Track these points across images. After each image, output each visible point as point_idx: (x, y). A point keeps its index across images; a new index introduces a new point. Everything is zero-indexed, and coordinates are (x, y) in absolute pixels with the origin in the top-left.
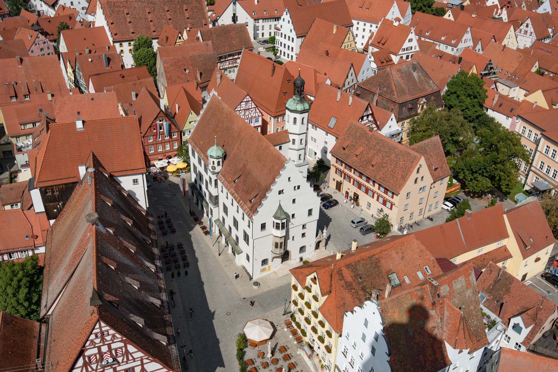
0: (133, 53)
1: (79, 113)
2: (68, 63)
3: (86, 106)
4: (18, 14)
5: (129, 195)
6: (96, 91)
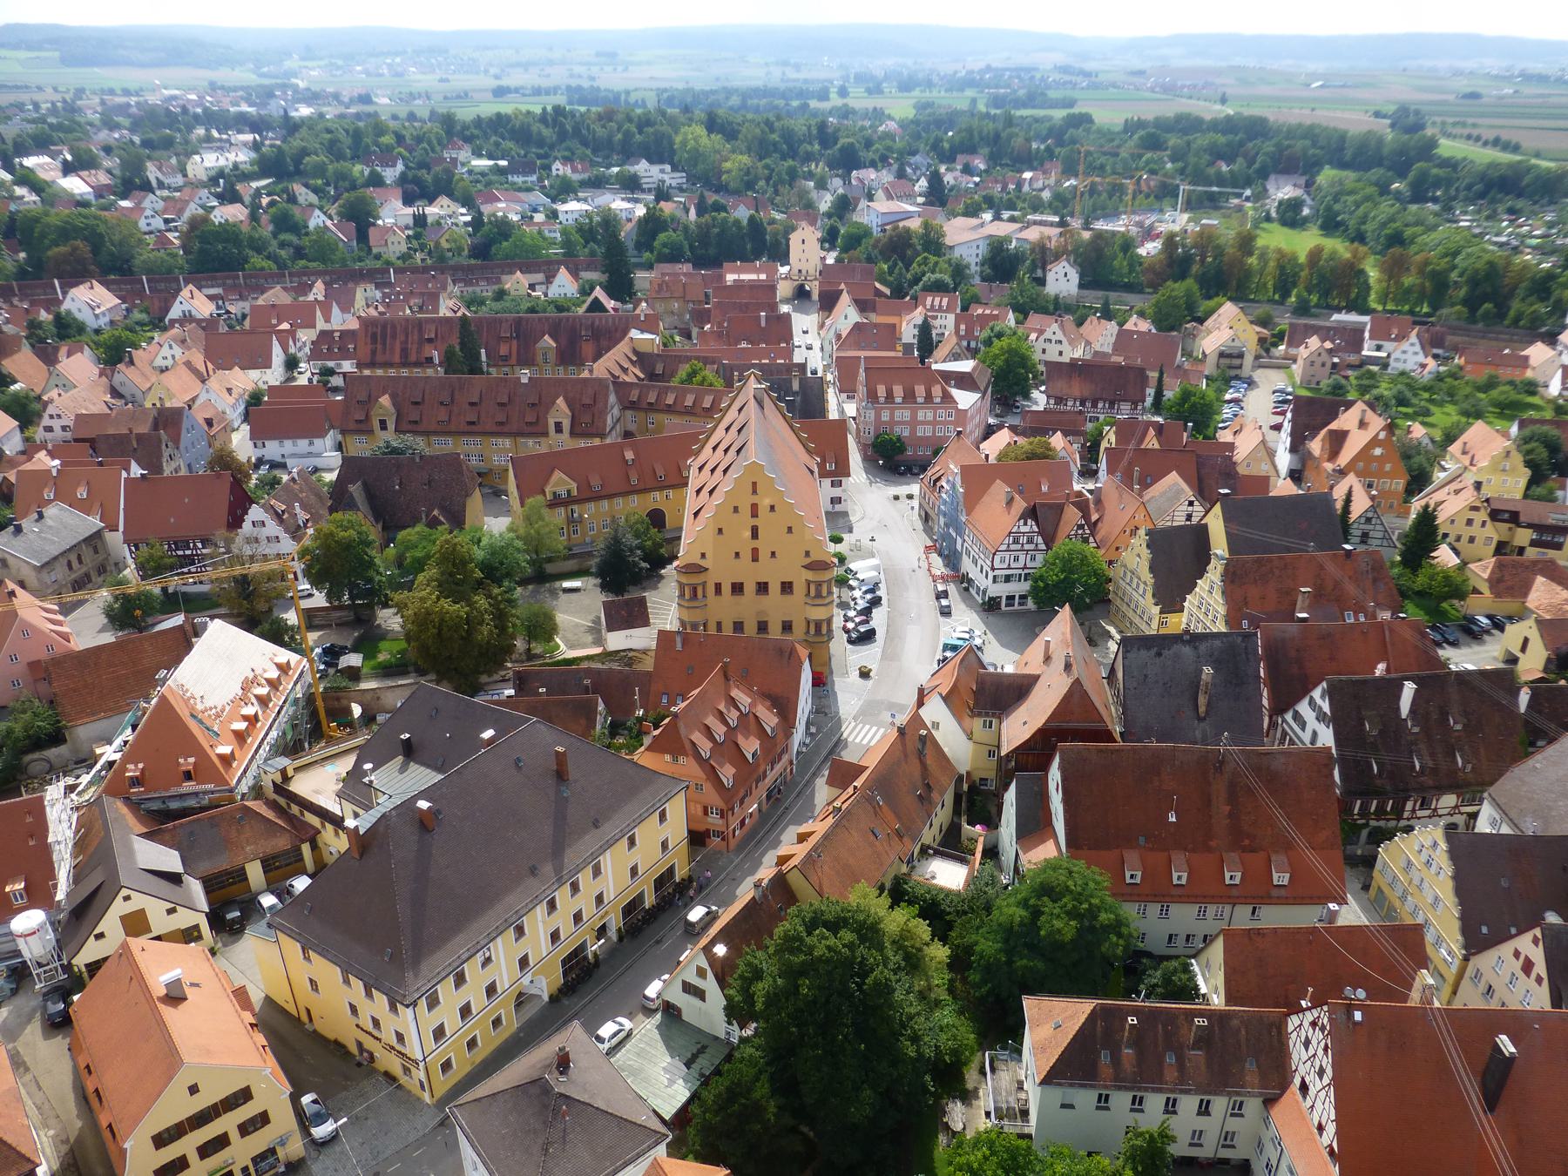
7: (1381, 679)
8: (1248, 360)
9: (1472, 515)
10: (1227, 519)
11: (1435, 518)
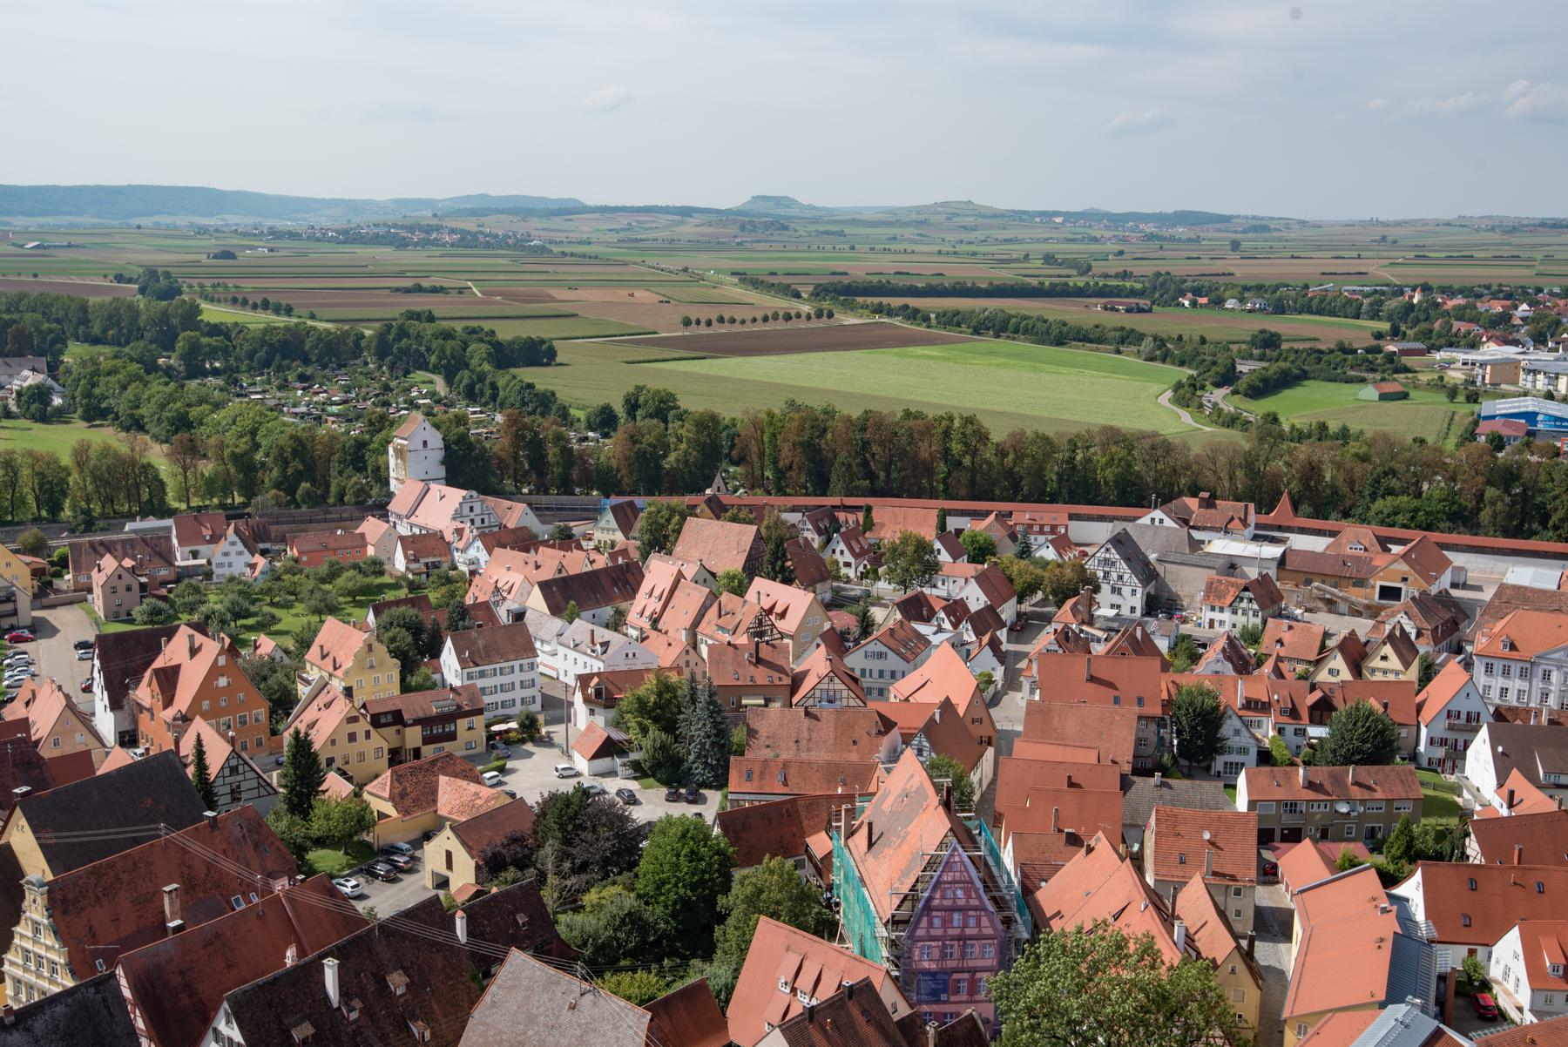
7: (295, 968)
8: (24, 601)
9: (352, 728)
10: (35, 829)
11: (310, 744)
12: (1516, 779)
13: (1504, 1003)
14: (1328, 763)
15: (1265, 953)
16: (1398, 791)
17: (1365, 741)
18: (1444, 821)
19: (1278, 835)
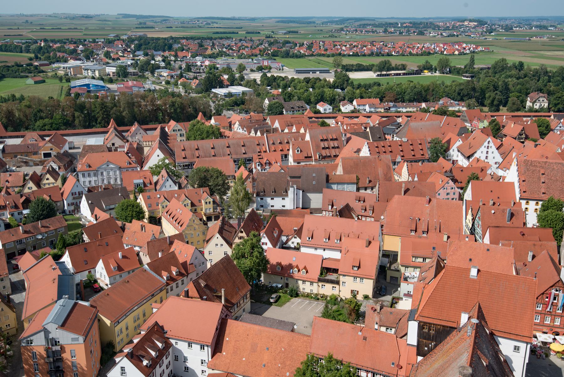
0: (538, 213)
1: (470, 260)
2: (470, 211)
3: (480, 256)
4: (435, 161)
5: (505, 361)
6: (491, 243)
12: (97, 211)
13: (102, 285)
14: (32, 222)
15: (17, 298)
16: (58, 225)
17: (43, 211)
18: (77, 231)
19: (17, 253)
